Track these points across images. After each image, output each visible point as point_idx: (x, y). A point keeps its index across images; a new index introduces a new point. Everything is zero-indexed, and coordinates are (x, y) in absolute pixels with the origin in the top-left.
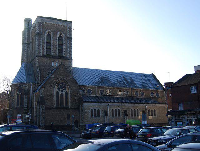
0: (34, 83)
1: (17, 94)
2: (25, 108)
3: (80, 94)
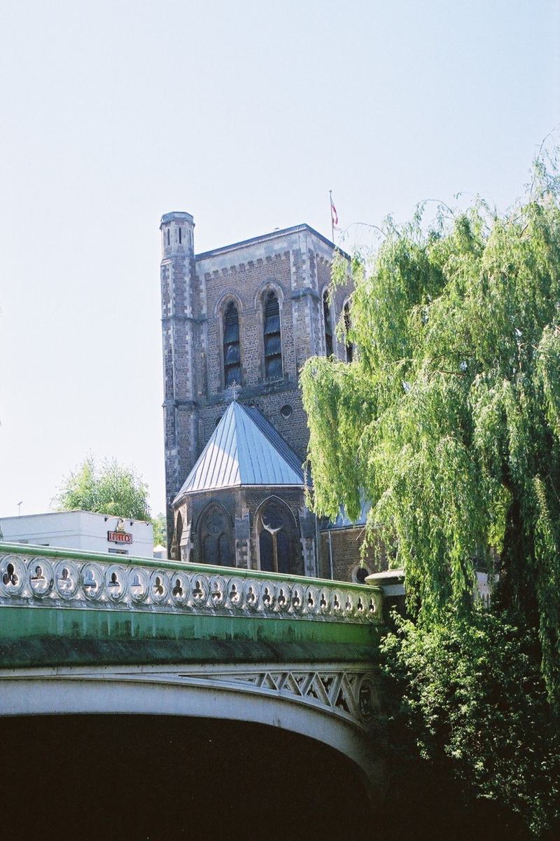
1: (264, 534)
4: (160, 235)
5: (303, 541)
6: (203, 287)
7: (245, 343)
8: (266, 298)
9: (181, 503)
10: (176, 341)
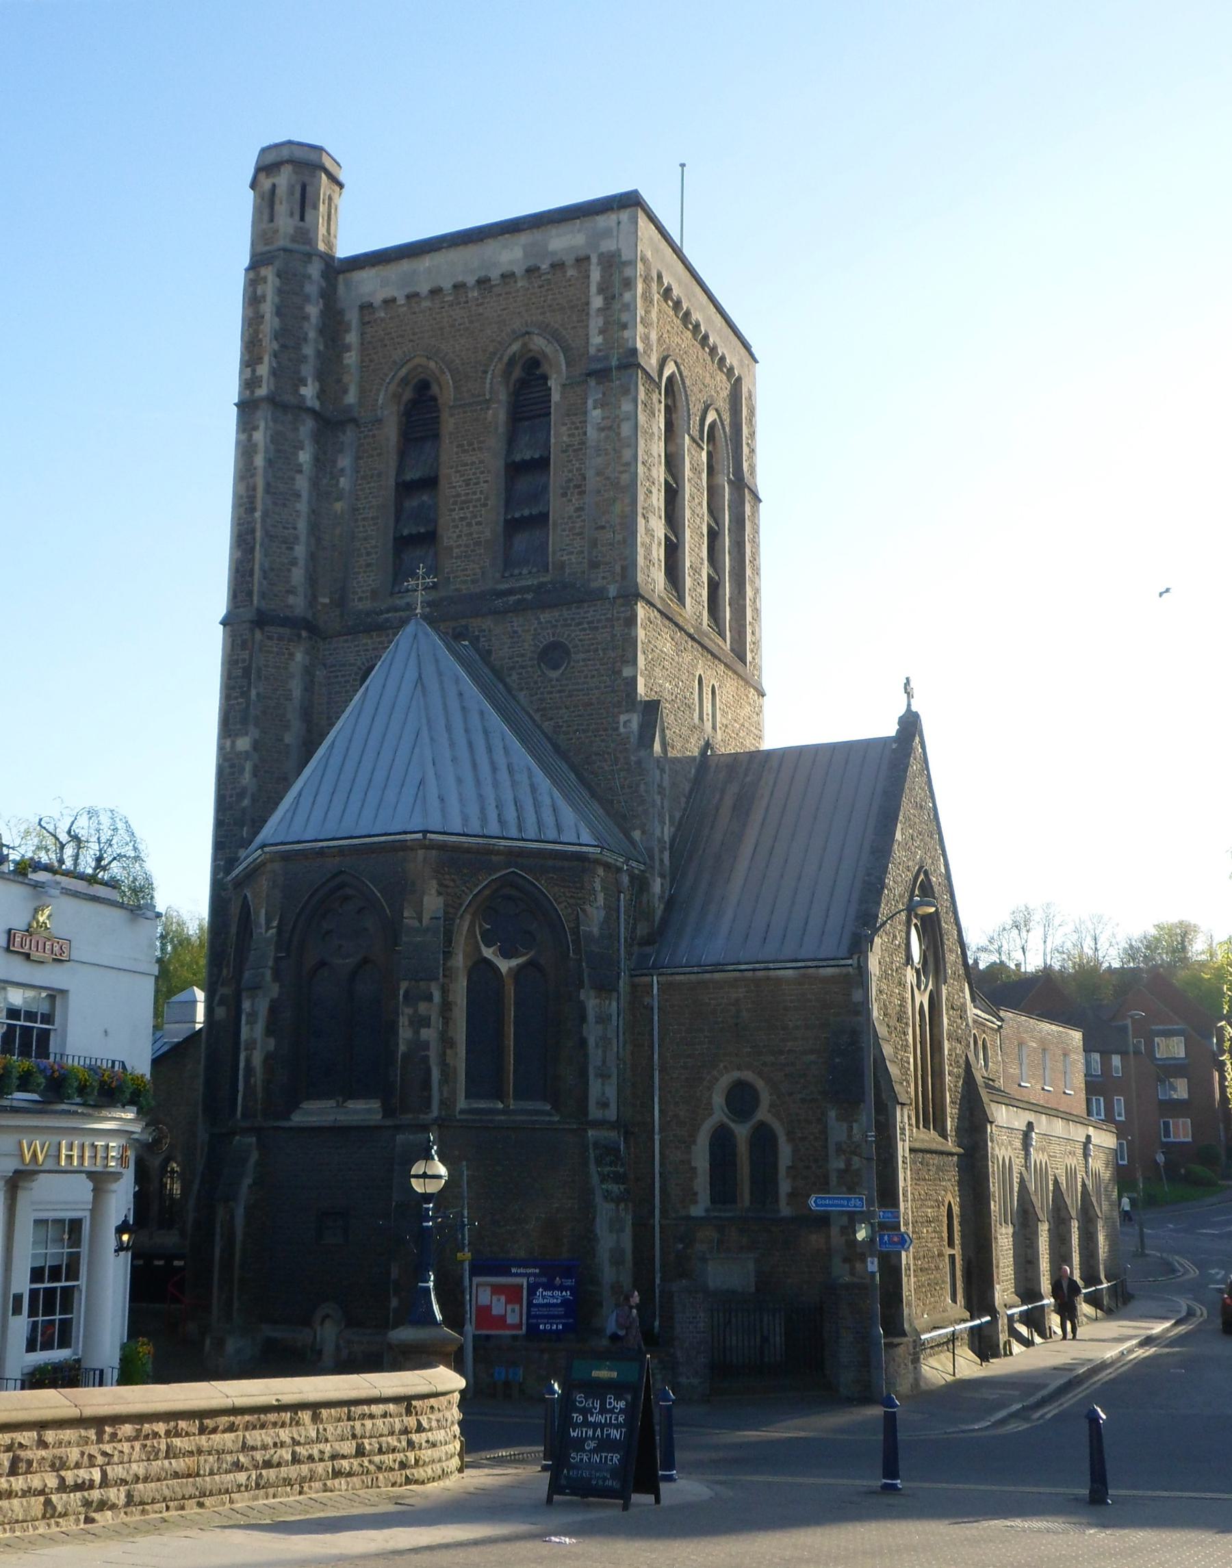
1: (481, 968)
2: (600, 1124)
4: (246, 201)
5: (592, 1003)
6: (352, 338)
7: (452, 482)
8: (517, 373)
9: (252, 873)
10: (270, 463)
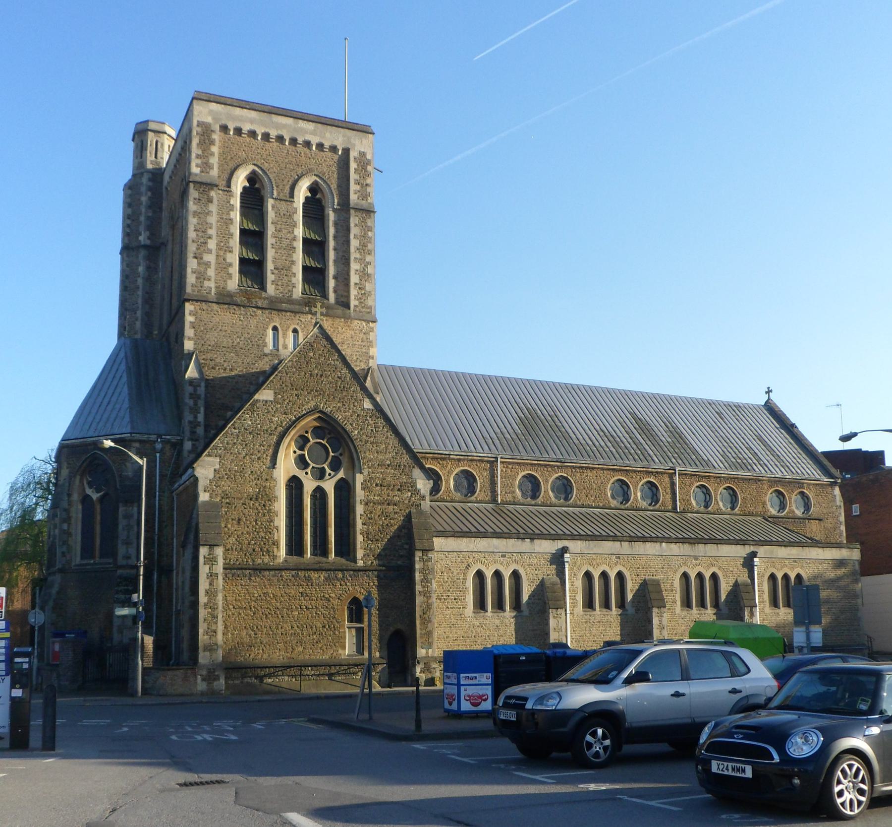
0: (174, 439)
1: (86, 499)
3: (416, 492)
